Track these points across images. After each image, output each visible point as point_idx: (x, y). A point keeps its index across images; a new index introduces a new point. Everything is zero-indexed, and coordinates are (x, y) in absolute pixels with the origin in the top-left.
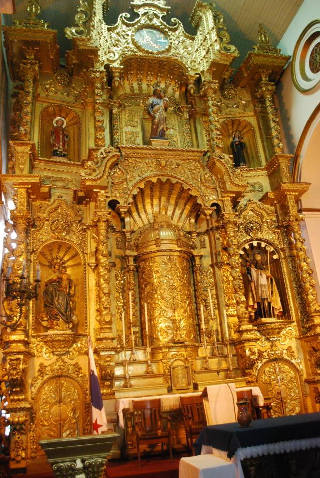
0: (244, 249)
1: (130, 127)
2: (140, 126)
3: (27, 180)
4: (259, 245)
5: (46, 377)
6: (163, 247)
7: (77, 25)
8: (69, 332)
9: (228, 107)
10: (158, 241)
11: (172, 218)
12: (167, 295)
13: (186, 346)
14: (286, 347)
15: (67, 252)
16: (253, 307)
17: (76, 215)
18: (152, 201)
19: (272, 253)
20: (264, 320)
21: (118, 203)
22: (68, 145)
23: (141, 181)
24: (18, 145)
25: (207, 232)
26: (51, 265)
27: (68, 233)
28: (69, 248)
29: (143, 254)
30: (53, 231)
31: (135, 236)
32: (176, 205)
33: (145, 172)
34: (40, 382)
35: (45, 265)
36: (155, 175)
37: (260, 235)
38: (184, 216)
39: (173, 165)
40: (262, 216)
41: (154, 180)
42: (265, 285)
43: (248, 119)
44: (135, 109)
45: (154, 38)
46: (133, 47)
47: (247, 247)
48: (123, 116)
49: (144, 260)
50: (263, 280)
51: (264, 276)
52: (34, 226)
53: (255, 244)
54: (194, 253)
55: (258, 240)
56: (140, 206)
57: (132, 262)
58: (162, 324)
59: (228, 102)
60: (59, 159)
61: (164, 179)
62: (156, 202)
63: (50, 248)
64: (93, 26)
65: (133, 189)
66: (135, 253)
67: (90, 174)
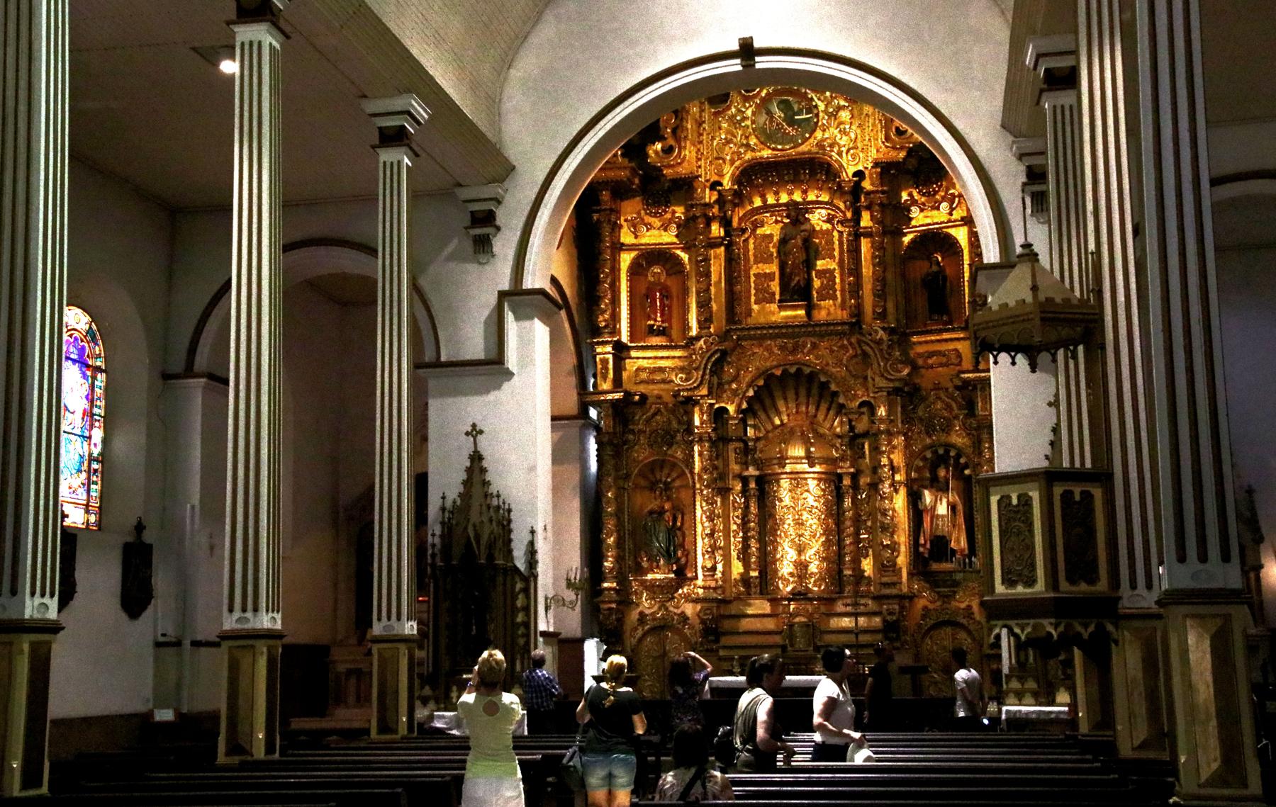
0: (924, 459)
1: (760, 265)
2: (776, 261)
3: (609, 397)
4: (947, 452)
5: (647, 627)
6: (788, 468)
7: (661, 139)
8: (672, 575)
9: (922, 210)
10: (782, 461)
11: (815, 416)
12: (791, 531)
13: (811, 600)
14: (963, 606)
15: (672, 470)
16: (924, 545)
17: (679, 422)
18: (784, 393)
19: (966, 466)
20: (935, 566)
21: (726, 410)
22: (670, 307)
23: (757, 378)
24: (599, 343)
25: (865, 435)
26: (652, 487)
27: (670, 445)
28: (674, 465)
29: (766, 475)
30: (651, 446)
31: (760, 445)
32: (821, 397)
33: (766, 360)
34: (640, 632)
35: (645, 487)
36: (777, 367)
37: (943, 438)
38: (832, 413)
39: (805, 346)
40: (952, 409)
41: (778, 372)
42: (943, 516)
43: (952, 231)
44: (768, 232)
45: (790, 113)
46: (753, 141)
47: (929, 455)
48: (751, 246)
49: (770, 482)
50: (942, 509)
51: (945, 501)
52: (625, 443)
53: (941, 451)
54: (839, 471)
55: (941, 445)
56: (768, 402)
57: (753, 485)
58: (786, 568)
59: (923, 199)
60: (656, 341)
61: (793, 370)
62: (791, 394)
63: (653, 467)
64: (686, 137)
65: (747, 390)
66: (757, 473)
67: (687, 380)
